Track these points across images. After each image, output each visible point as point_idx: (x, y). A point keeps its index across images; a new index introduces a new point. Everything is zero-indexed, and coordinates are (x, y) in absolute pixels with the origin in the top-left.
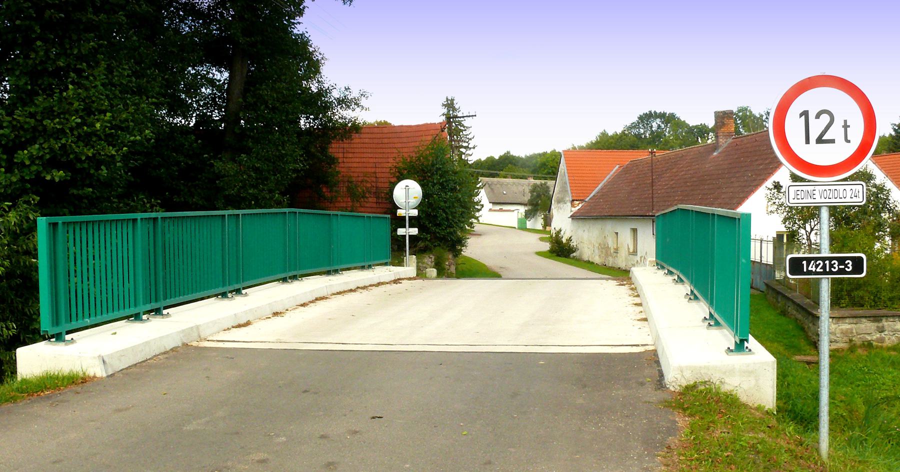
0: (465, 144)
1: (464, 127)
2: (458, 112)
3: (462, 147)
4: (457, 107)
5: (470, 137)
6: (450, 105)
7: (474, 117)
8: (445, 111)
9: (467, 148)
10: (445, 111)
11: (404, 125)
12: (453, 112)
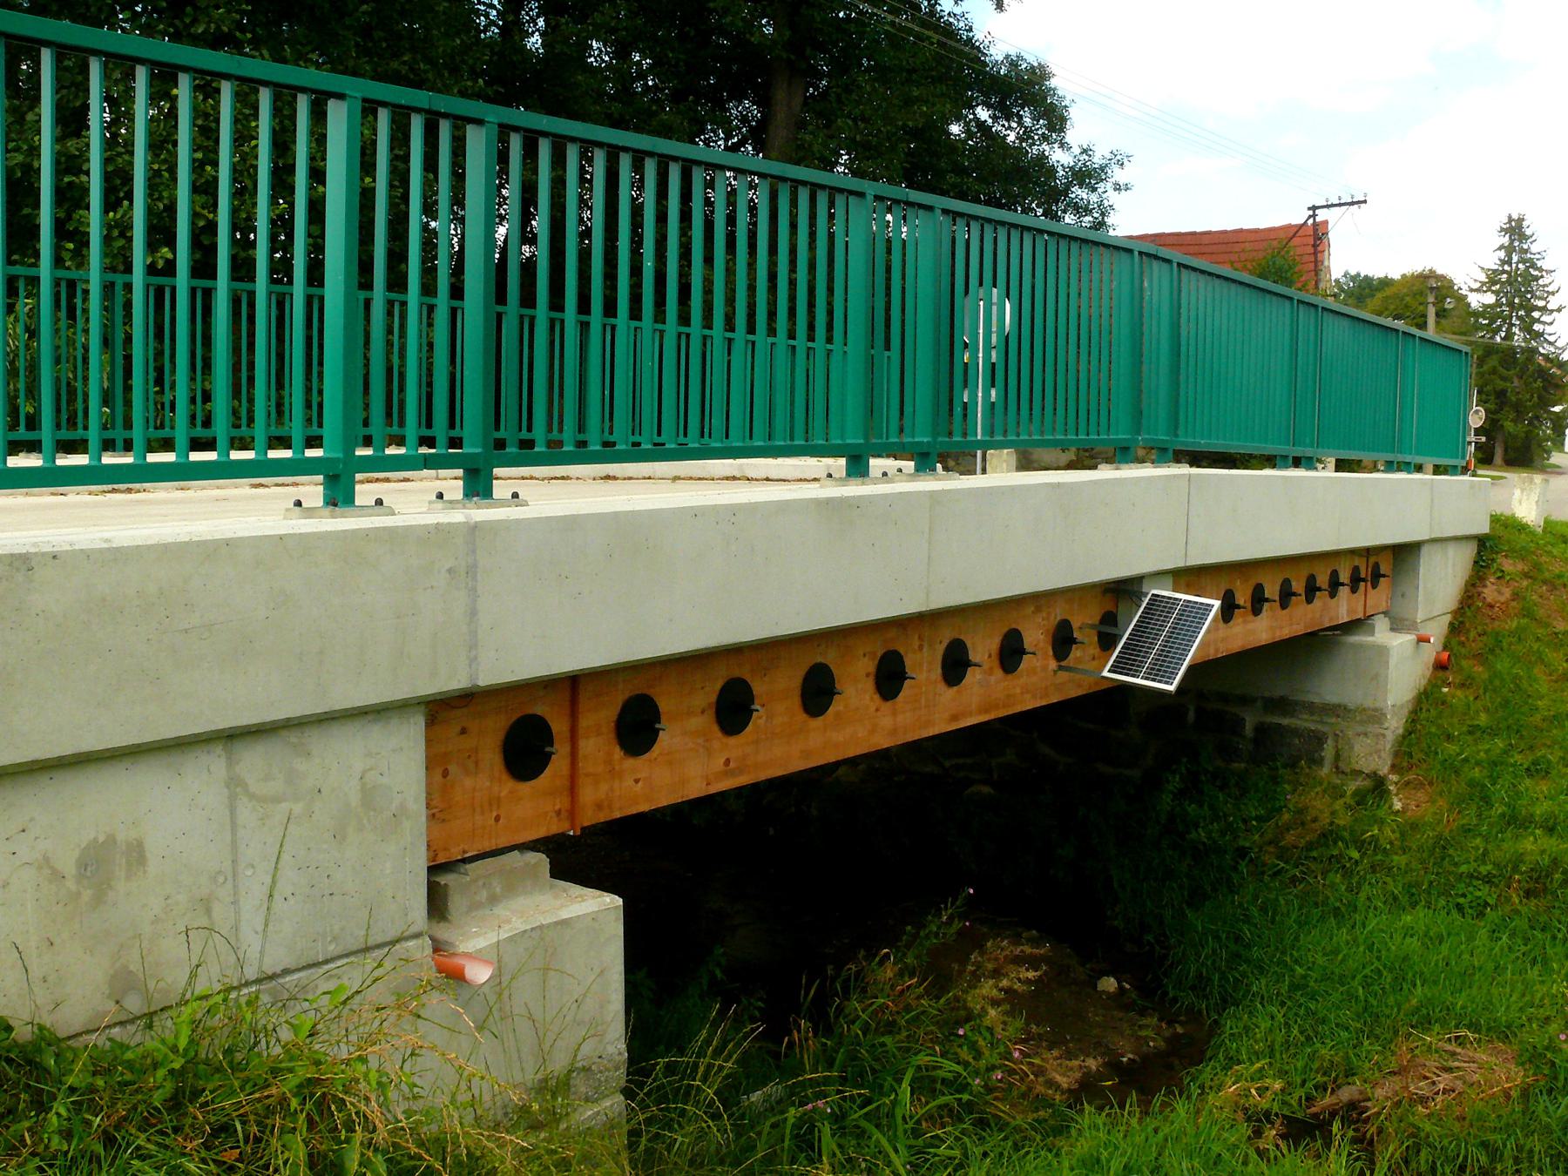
0: (1541, 303)
1: (1540, 269)
2: (1531, 243)
3: (1537, 308)
4: (1528, 232)
5: (1550, 289)
6: (1515, 230)
7: (1362, 205)
8: (1506, 240)
9: (1544, 309)
10: (1506, 240)
11: (1245, 227)
12: (1521, 242)
